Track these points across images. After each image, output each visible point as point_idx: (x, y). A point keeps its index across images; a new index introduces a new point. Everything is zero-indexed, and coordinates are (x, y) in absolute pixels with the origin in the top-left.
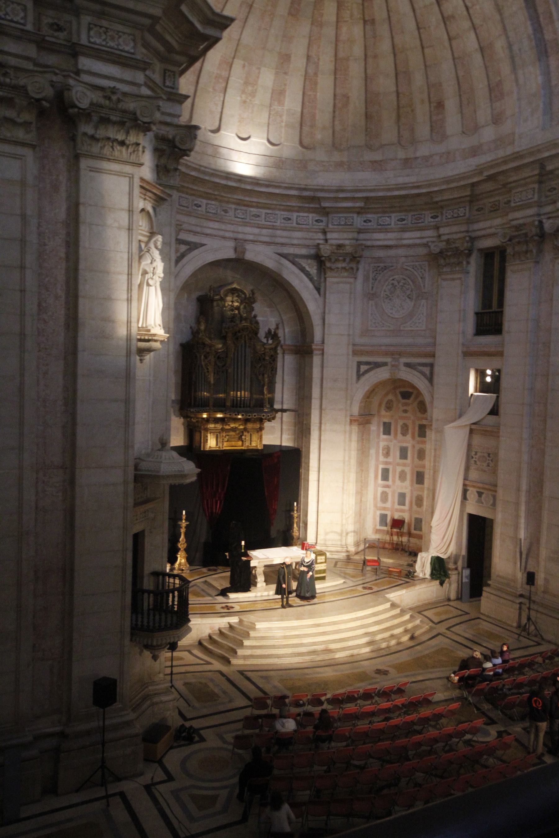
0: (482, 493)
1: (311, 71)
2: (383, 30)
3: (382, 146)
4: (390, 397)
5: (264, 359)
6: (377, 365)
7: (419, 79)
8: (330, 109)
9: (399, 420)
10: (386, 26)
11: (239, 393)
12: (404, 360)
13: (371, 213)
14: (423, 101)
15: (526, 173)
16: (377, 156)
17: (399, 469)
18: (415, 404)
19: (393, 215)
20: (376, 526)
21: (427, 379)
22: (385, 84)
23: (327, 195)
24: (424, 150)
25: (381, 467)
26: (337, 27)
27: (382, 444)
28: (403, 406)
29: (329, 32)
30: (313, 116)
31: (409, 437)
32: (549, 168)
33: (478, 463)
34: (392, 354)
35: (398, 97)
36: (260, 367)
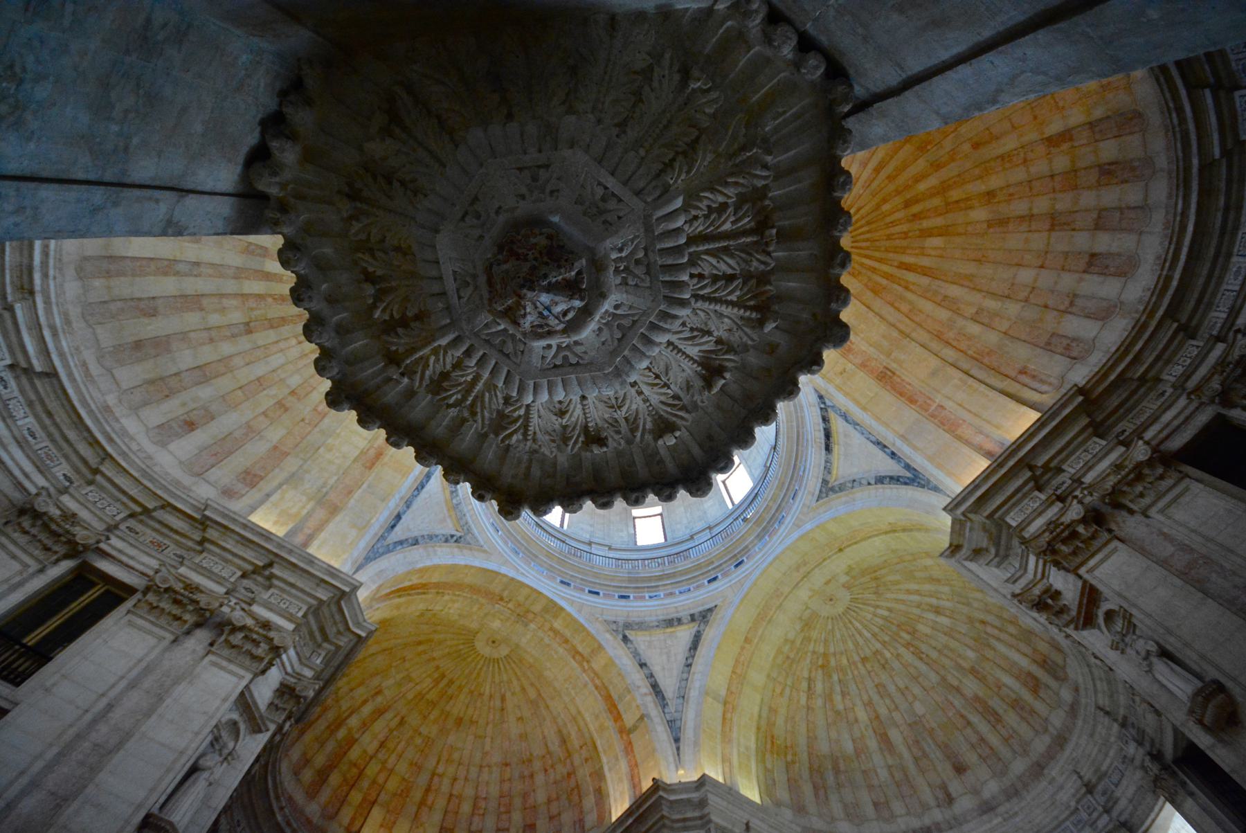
1: (181, 267)
2: (244, 343)
3: (110, 371)
7: (205, 393)
8: (138, 295)
10: (248, 346)
13: (19, 385)
14: (184, 404)
15: (249, 554)
16: (95, 369)
19: (31, 419)
22: (185, 359)
23: (41, 312)
24: (131, 425)
26: (235, 295)
29: (230, 286)
30: (120, 274)
32: (276, 571)
35: (175, 374)
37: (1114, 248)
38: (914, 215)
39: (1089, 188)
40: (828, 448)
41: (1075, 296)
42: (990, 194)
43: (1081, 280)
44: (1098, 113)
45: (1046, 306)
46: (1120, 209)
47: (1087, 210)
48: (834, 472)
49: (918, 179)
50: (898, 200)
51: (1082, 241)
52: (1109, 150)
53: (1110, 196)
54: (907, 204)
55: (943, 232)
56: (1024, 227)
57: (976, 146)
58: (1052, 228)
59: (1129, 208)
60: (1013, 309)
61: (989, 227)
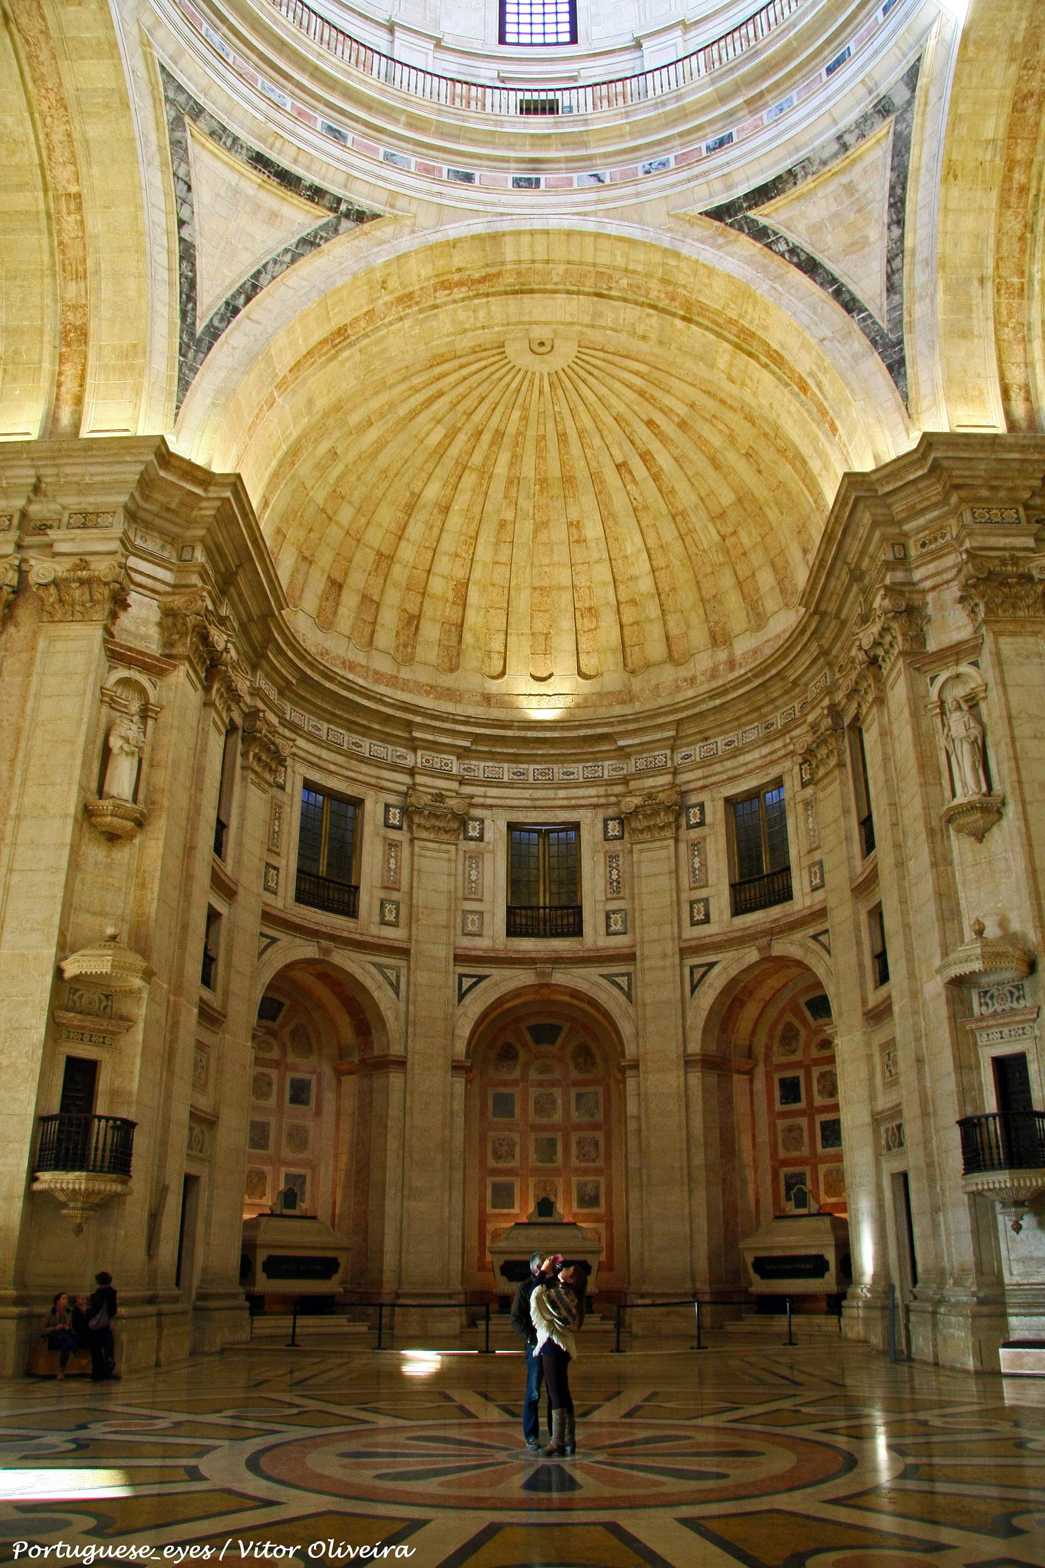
37: (342, 610)
38: (481, 433)
39: (402, 600)
40: (259, 161)
41: (311, 563)
42: (446, 510)
43: (323, 571)
44: (468, 638)
45: (311, 530)
46: (374, 623)
47: (382, 591)
48: (211, 144)
49: (515, 460)
50: (512, 429)
51: (356, 580)
52: (430, 631)
53: (389, 618)
54: (499, 435)
55: (440, 451)
56: (393, 527)
57: (502, 524)
58: (380, 554)
59: (373, 632)
60: (320, 496)
61: (413, 494)
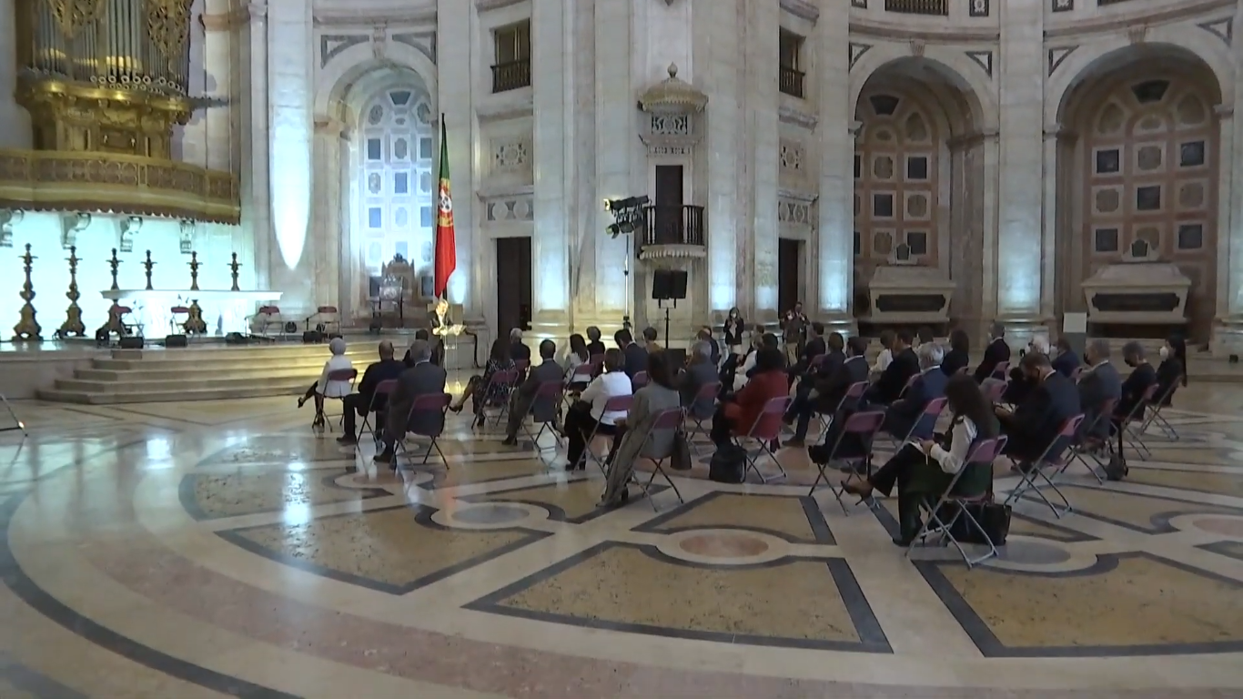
0: (514, 203)
4: (377, 101)
5: (166, 17)
6: (353, 40)
9: (392, 136)
11: (121, 59)
12: (391, 31)
17: (396, 207)
18: (415, 110)
20: (365, 297)
21: (428, 56)
25: (367, 207)
27: (367, 173)
28: (396, 114)
31: (408, 158)
33: (506, 162)
34: (372, 21)
36: (160, 28)
